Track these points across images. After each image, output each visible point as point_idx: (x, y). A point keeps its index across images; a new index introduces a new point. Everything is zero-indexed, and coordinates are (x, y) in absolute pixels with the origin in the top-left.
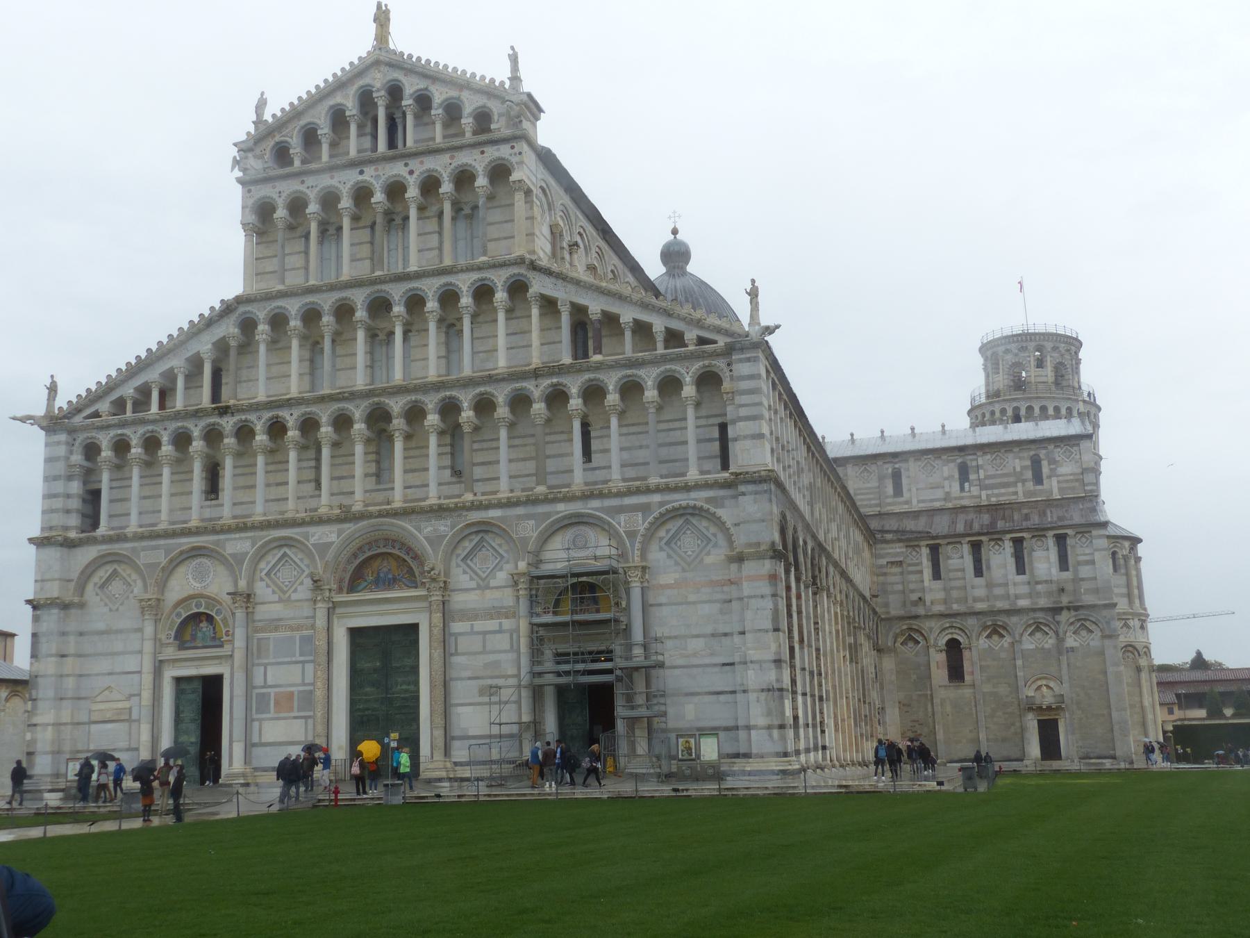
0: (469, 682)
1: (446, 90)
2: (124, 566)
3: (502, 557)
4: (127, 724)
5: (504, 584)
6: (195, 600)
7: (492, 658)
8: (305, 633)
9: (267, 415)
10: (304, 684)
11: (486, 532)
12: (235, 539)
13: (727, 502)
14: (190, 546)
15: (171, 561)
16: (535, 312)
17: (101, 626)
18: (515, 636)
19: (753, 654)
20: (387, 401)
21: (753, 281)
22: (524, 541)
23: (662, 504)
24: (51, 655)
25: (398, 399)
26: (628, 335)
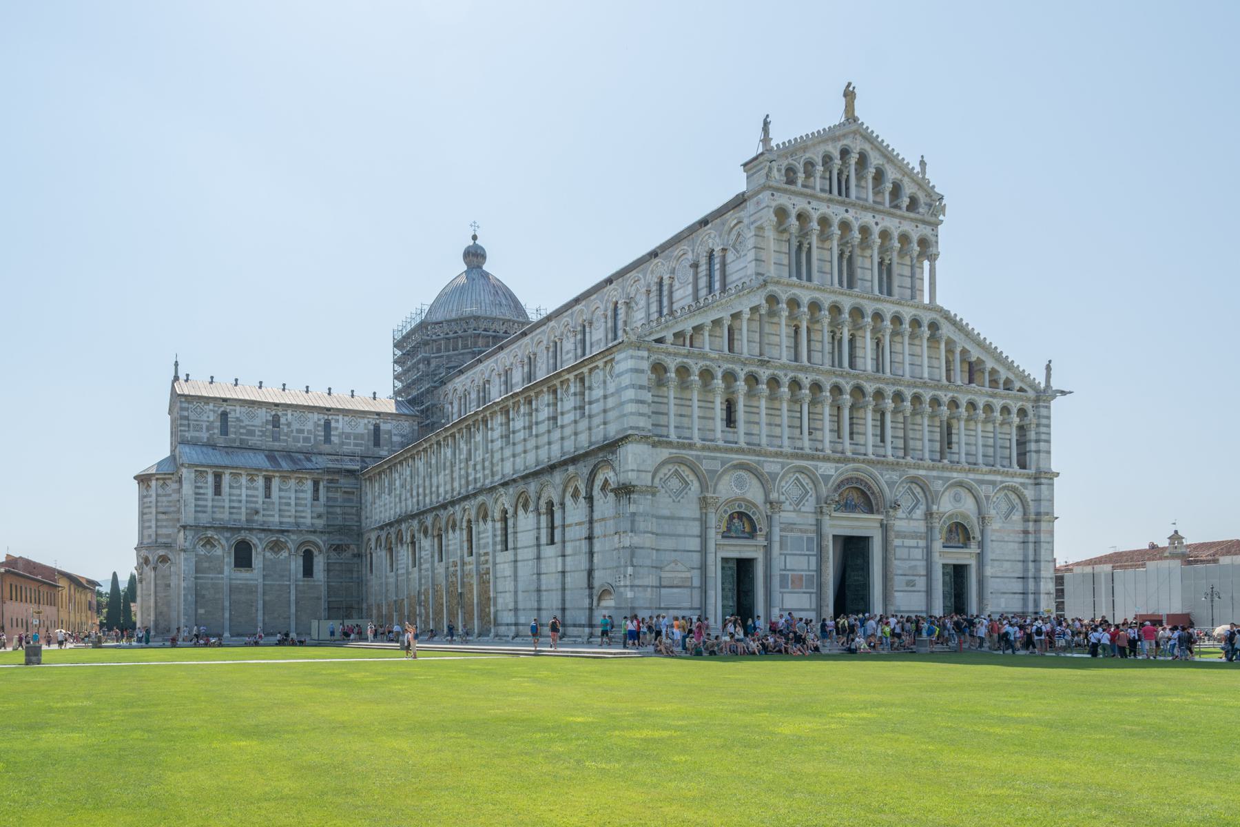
0: (903, 577)
2: (683, 468)
3: (918, 501)
4: (689, 590)
5: (919, 518)
6: (738, 503)
7: (913, 563)
8: (810, 535)
10: (809, 570)
13: (1030, 487)
14: (738, 461)
17: (666, 512)
19: (1043, 574)
22: (937, 492)
23: (1002, 482)
24: (648, 532)
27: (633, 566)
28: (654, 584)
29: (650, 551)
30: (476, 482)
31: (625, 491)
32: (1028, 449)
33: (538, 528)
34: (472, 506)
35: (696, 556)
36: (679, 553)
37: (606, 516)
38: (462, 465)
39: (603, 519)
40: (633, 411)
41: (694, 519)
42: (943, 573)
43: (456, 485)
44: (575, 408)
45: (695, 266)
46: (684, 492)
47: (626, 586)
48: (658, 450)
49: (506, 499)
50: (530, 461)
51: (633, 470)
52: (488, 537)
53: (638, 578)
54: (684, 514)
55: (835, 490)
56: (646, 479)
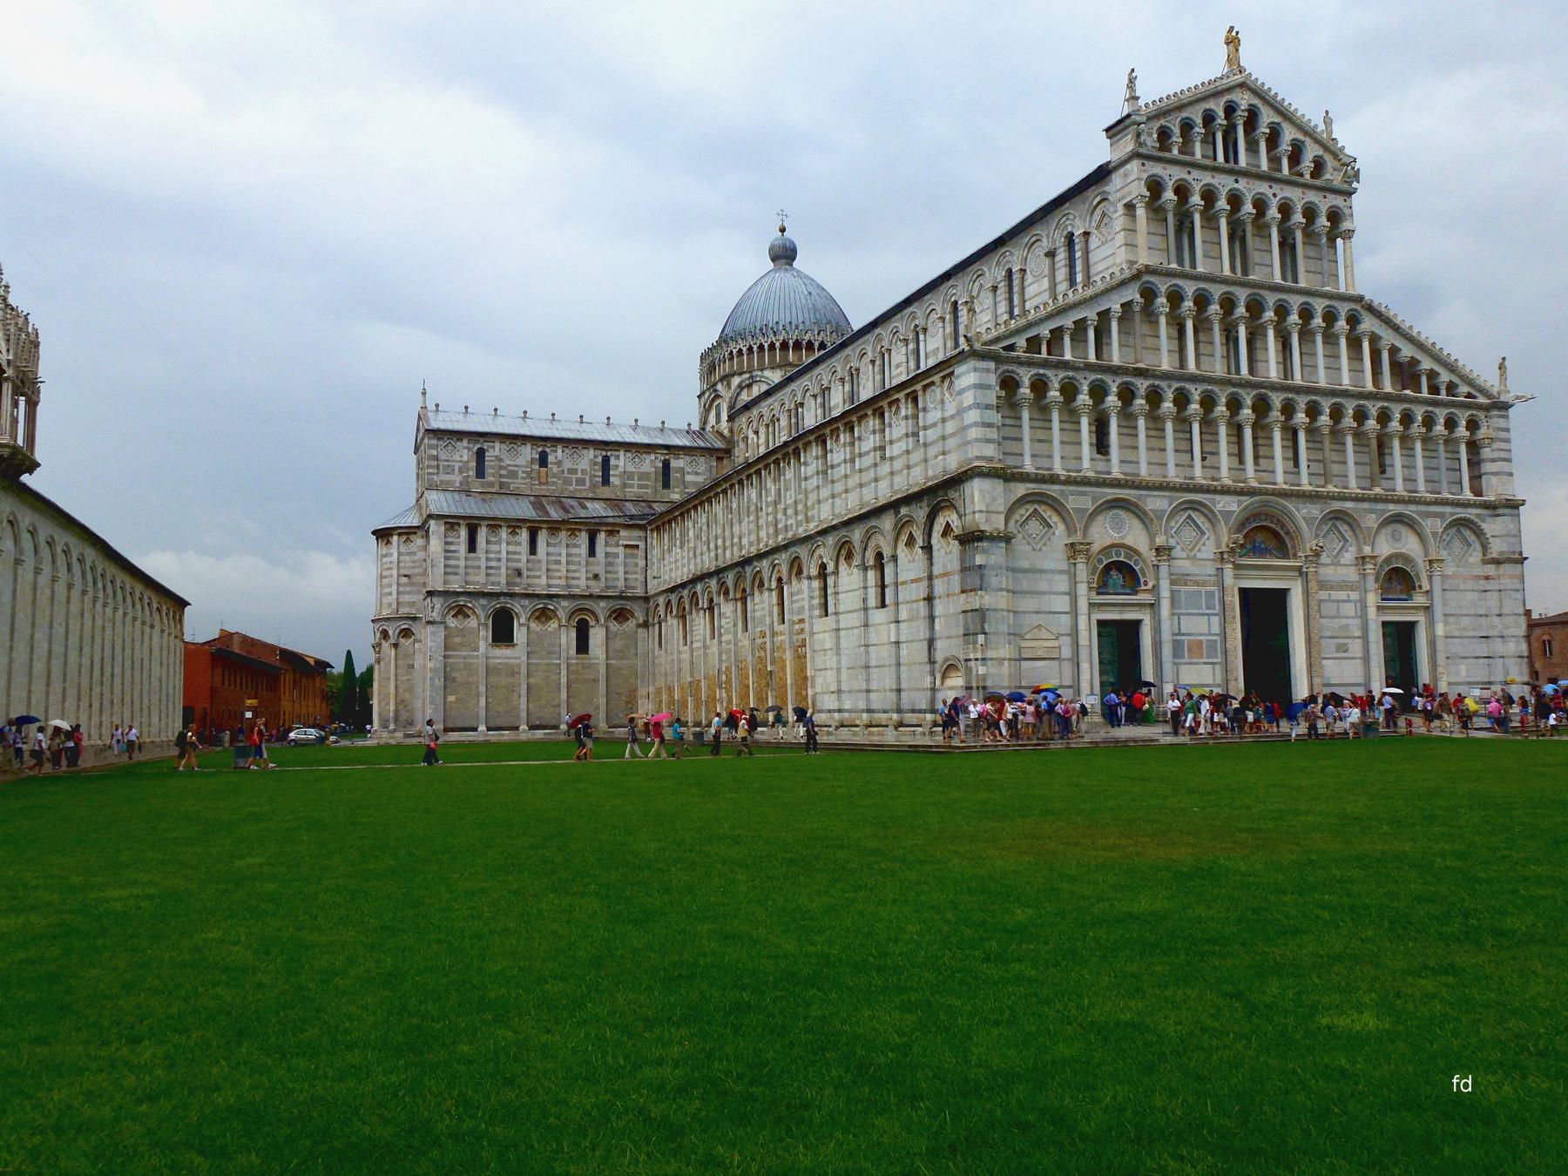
1: (1294, 131)
2: (1044, 507)
4: (1057, 662)
9: (1176, 385)
11: (1336, 518)
12: (1155, 496)
13: (1488, 519)
15: (1096, 508)
16: (1366, 345)
18: (1358, 605)
20: (1270, 394)
21: (1504, 359)
22: (1369, 529)
23: (1452, 514)
24: (1001, 590)
25: (1278, 394)
26: (1424, 379)
27: (985, 634)
28: (1012, 657)
29: (1005, 613)
30: (786, 530)
31: (970, 538)
32: (1483, 471)
33: (865, 588)
34: (783, 558)
35: (1065, 620)
36: (1042, 616)
37: (949, 570)
38: (770, 510)
39: (945, 575)
40: (979, 437)
41: (1061, 572)
42: (1384, 634)
43: (763, 534)
44: (907, 435)
45: (1051, 254)
46: (1047, 537)
47: (977, 659)
48: (1012, 485)
49: (826, 552)
50: (852, 504)
51: (981, 511)
52: (803, 599)
53: (991, 648)
54: (1049, 565)
55: (1238, 531)
56: (998, 523)
